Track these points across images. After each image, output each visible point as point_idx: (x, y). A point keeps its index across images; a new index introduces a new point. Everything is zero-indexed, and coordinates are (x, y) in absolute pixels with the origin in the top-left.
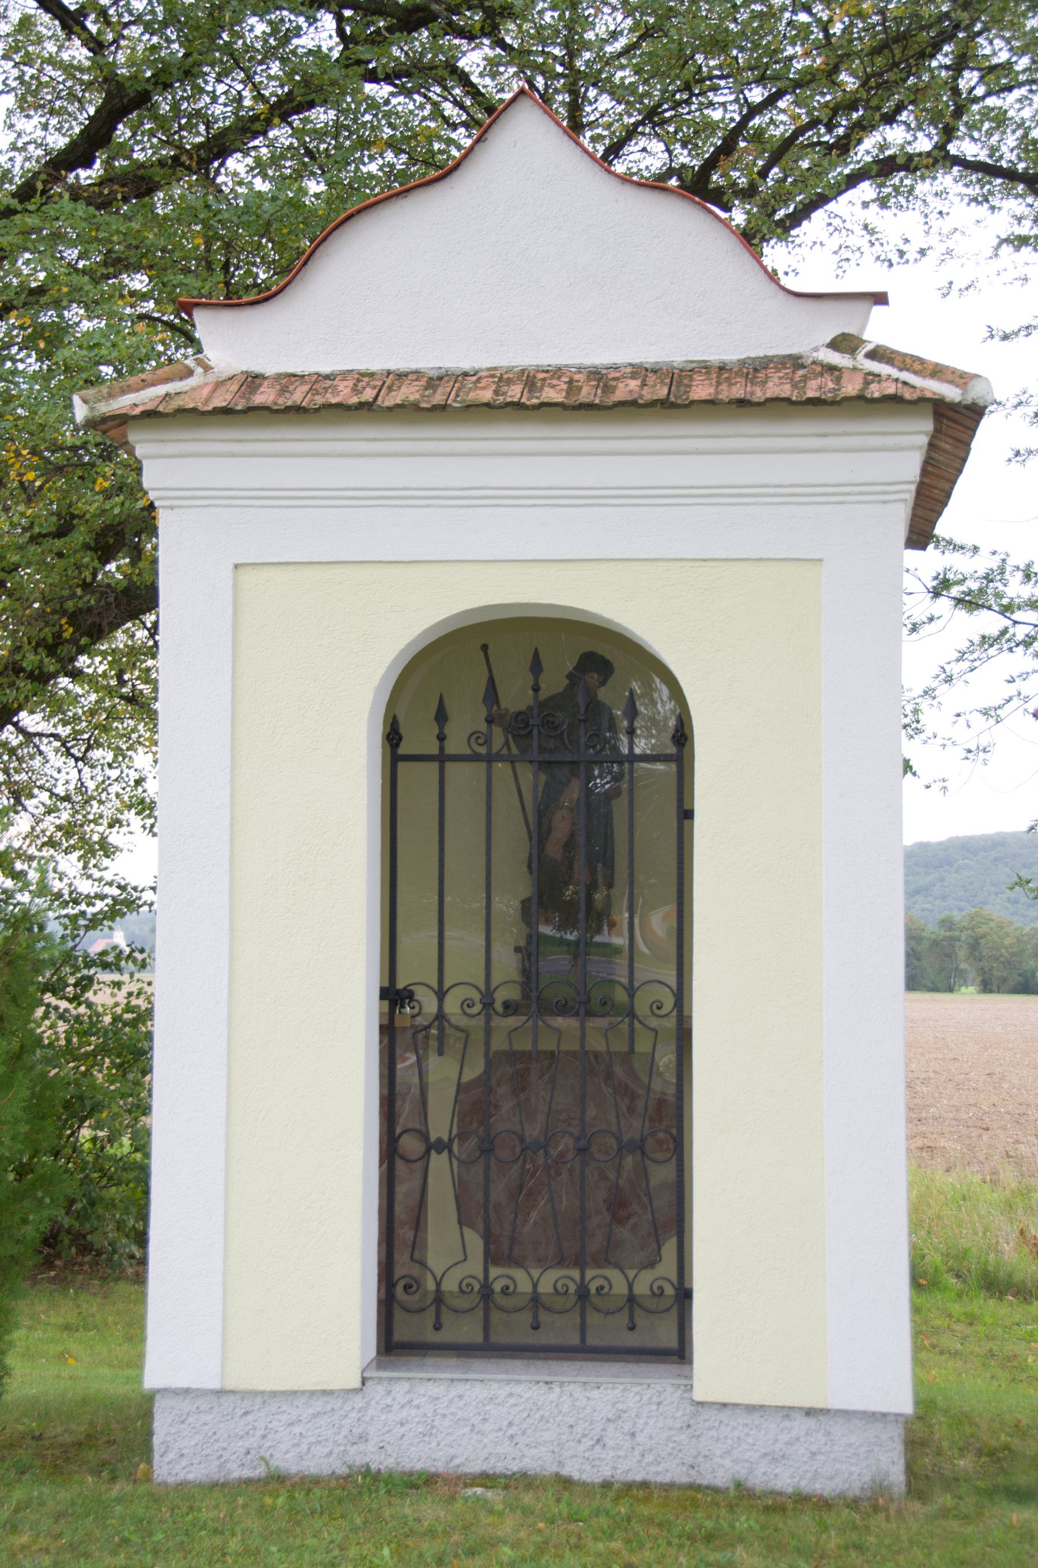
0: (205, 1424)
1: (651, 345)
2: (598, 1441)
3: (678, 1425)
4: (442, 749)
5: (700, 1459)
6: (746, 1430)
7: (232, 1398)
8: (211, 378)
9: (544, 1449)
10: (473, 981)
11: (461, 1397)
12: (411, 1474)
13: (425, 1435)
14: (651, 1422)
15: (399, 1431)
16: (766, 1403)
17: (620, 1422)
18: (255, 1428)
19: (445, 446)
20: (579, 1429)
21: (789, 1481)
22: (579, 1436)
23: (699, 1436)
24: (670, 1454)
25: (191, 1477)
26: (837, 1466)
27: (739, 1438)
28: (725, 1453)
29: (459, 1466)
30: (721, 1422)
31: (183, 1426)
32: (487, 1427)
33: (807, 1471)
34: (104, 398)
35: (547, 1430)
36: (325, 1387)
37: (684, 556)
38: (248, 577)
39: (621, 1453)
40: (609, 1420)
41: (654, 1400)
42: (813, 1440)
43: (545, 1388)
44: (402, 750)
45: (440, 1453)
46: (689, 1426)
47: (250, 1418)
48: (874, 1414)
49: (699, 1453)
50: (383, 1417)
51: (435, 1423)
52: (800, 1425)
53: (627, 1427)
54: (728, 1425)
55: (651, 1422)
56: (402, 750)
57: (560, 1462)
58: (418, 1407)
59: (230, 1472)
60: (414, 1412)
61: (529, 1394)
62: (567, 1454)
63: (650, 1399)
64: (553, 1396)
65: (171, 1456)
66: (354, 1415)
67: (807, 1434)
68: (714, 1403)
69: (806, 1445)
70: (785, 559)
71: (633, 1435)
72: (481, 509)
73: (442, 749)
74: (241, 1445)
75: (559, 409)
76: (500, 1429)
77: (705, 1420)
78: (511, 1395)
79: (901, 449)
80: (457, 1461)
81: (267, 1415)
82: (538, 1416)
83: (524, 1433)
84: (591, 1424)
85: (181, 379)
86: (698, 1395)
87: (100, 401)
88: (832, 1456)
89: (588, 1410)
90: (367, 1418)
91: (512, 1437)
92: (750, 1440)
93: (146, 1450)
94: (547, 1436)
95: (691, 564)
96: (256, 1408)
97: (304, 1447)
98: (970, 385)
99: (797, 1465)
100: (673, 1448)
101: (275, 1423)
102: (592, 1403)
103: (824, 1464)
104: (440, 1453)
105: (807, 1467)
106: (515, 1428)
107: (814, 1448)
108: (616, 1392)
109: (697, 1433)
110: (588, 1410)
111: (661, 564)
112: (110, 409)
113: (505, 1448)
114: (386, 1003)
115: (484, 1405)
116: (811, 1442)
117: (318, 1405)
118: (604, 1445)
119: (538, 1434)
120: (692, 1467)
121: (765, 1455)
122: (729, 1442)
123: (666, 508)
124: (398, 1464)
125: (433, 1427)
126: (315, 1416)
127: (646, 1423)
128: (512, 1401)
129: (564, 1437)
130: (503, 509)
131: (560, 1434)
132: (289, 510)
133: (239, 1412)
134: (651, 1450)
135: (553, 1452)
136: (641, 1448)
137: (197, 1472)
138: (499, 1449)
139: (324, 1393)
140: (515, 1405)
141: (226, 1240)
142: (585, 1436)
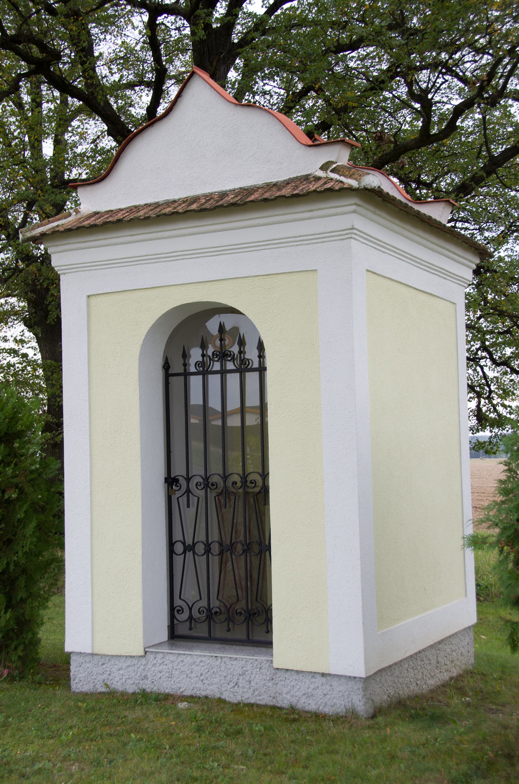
0: (88, 668)
1: (250, 178)
2: (236, 684)
3: (268, 679)
4: (185, 370)
5: (277, 695)
6: (296, 682)
7: (98, 657)
8: (79, 216)
9: (214, 686)
10: (256, 471)
11: (182, 661)
12: (159, 694)
13: (169, 678)
14: (257, 676)
15: (159, 675)
16: (391, 664)
17: (245, 676)
18: (106, 671)
19: (159, 235)
20: (228, 678)
21: (315, 707)
22: (228, 682)
23: (277, 684)
24: (265, 692)
25: (83, 690)
26: (335, 701)
27: (293, 686)
28: (288, 692)
29: (182, 692)
30: (286, 678)
31: (81, 668)
32: (193, 675)
33: (322, 703)
34: (29, 230)
35: (216, 678)
36: (130, 655)
37: (259, 274)
38: (93, 300)
39: (245, 690)
40: (240, 675)
41: (258, 666)
42: (324, 688)
43: (215, 658)
44: (170, 372)
45: (175, 686)
46: (273, 679)
47: (104, 666)
48: (350, 677)
49: (277, 692)
50: (153, 669)
51: (173, 673)
52: (319, 680)
53: (247, 678)
54: (288, 679)
55: (257, 676)
56: (170, 372)
57: (221, 693)
58: (166, 665)
59: (98, 689)
60: (165, 667)
61: (208, 661)
62: (224, 689)
63: (257, 665)
64: (218, 663)
65: (77, 680)
66: (142, 667)
67: (322, 685)
68: (283, 669)
69: (322, 690)
70: (301, 271)
71: (250, 682)
72: (178, 261)
73: (185, 370)
74: (102, 677)
75: (193, 212)
76: (197, 677)
77: (279, 677)
78: (201, 661)
79: (344, 213)
80: (181, 690)
81: (111, 665)
82: (212, 672)
83: (207, 679)
84: (233, 676)
85: (65, 218)
86: (275, 665)
87: (27, 232)
88: (333, 696)
89: (232, 670)
90: (147, 669)
91: (202, 680)
92: (298, 687)
93: (68, 678)
94: (216, 680)
95: (262, 277)
96: (107, 662)
97: (124, 680)
98: (362, 180)
99: (318, 699)
100: (266, 689)
101: (113, 669)
102: (233, 666)
103: (329, 699)
104: (175, 686)
105: (322, 701)
106: (203, 676)
107: (325, 692)
108: (243, 662)
109: (276, 683)
110: (232, 670)
111: (250, 279)
112: (32, 234)
113: (200, 685)
114: (167, 484)
115: (191, 666)
116: (324, 690)
117: (129, 662)
118: (239, 686)
119: (212, 679)
120: (274, 698)
121: (304, 694)
122: (289, 687)
123: (251, 253)
124: (159, 689)
125: (172, 674)
126: (128, 666)
127: (255, 677)
128: (202, 664)
129: (222, 681)
130: (186, 260)
131: (221, 680)
132: (106, 270)
133: (100, 663)
134: (257, 689)
135: (218, 688)
136: (253, 688)
137: (86, 688)
138: (197, 686)
139: (132, 657)
140: (203, 666)
141: (92, 589)
142: (231, 681)
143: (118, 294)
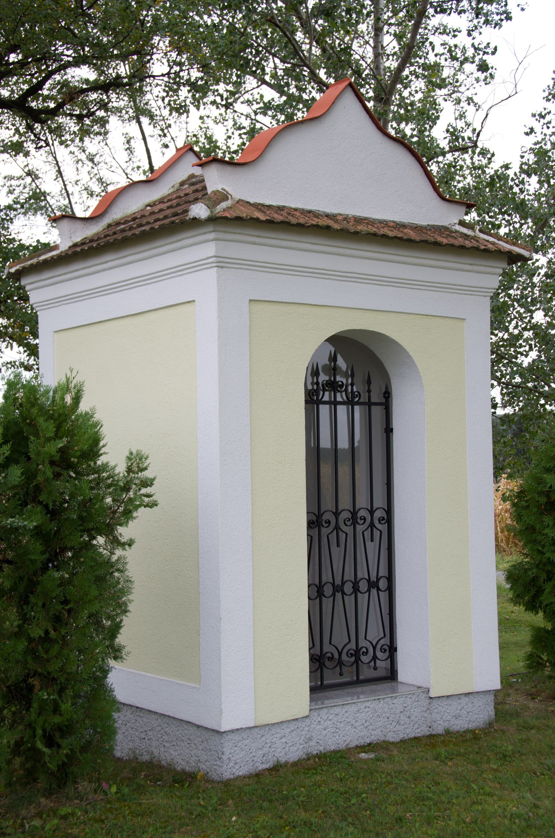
9: (378, 730)
25: (241, 773)
47: (263, 738)
52: (464, 700)
58: (331, 720)
59: (257, 767)
60: (329, 723)
64: (381, 705)
65: (231, 764)
97: (287, 748)
101: (275, 739)
107: (468, 710)
117: (292, 726)
128: (366, 710)
143: (282, 304)
